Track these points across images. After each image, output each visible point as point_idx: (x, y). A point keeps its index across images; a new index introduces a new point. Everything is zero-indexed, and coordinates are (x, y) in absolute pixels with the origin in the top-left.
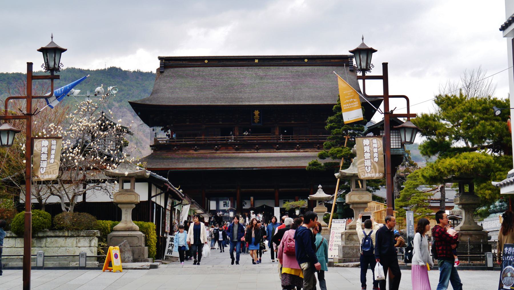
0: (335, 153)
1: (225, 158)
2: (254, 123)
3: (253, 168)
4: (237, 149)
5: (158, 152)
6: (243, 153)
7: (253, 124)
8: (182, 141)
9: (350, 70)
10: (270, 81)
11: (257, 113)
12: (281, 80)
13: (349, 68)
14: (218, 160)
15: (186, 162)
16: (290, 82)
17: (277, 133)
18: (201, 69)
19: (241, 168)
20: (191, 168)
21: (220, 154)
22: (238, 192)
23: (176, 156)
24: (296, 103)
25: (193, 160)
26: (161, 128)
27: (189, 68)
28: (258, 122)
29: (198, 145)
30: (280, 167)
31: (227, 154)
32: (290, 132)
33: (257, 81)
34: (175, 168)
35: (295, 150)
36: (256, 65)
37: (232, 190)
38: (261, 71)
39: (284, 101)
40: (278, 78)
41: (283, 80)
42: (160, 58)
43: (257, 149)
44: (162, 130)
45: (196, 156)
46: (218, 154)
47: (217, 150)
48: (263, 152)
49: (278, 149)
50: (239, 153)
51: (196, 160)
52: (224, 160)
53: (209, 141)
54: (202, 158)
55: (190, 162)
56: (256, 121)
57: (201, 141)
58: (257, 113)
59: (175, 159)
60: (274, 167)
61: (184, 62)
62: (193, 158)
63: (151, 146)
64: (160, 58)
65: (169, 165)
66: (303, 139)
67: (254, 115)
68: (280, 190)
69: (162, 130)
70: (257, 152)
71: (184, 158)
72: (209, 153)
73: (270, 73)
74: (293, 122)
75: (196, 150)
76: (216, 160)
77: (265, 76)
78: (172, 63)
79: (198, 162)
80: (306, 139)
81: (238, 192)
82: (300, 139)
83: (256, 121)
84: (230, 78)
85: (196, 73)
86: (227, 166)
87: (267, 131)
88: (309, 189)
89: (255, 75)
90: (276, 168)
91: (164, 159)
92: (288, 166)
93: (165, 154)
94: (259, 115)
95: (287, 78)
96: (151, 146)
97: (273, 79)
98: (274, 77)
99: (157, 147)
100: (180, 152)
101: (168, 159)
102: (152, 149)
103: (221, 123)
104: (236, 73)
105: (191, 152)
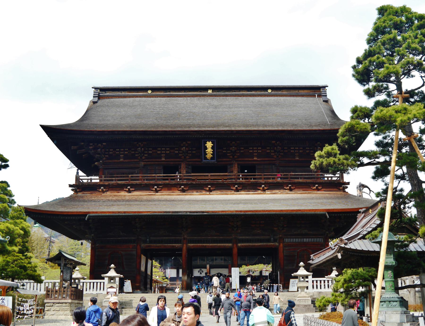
0: (390, 116)
1: (166, 200)
2: (206, 158)
3: (203, 212)
4: (183, 191)
5: (80, 194)
6: (191, 195)
7: (204, 161)
8: (113, 180)
9: (324, 101)
10: (227, 110)
11: (209, 145)
12: (241, 109)
13: (321, 99)
14: (157, 203)
15: (113, 205)
16: (251, 110)
17: (235, 172)
18: (144, 99)
19: (186, 212)
20: (119, 212)
21: (160, 197)
22: (184, 248)
23: (102, 198)
24: (261, 128)
25: (124, 203)
27: (129, 99)
28: (212, 158)
29: (132, 186)
30: (241, 211)
32: (252, 169)
33: (210, 110)
34: (96, 212)
35: (260, 192)
36: (210, 95)
37: (177, 245)
38: (216, 101)
39: (244, 126)
40: (236, 107)
41: (243, 109)
45: (127, 198)
46: (159, 196)
47: (157, 191)
50: (185, 195)
51: (127, 203)
52: (164, 203)
53: (147, 180)
54: (136, 200)
55: (118, 205)
56: (209, 156)
57: (138, 180)
58: (209, 145)
59: (99, 201)
60: (233, 211)
61: (123, 93)
62: (123, 201)
63: (70, 186)
64: (96, 88)
65: (89, 208)
66: (269, 179)
67: (206, 148)
68: (239, 245)
71: (112, 200)
72: (146, 195)
73: (227, 103)
74: (255, 159)
75: (129, 191)
76: (154, 203)
77: (221, 105)
79: (130, 205)
80: (273, 178)
81: (184, 248)
82: (265, 179)
83: (209, 156)
84: (177, 107)
85: (136, 103)
86: (168, 210)
87: (223, 169)
89: (208, 105)
90: (235, 213)
91: (84, 201)
92: (252, 209)
93: (87, 195)
94: (213, 148)
95: (248, 107)
96: (70, 186)
97: (230, 108)
98: (231, 106)
99: (79, 187)
100: (108, 193)
101: (91, 201)
102: (72, 190)
103: (163, 159)
104: (185, 103)
105: (123, 193)
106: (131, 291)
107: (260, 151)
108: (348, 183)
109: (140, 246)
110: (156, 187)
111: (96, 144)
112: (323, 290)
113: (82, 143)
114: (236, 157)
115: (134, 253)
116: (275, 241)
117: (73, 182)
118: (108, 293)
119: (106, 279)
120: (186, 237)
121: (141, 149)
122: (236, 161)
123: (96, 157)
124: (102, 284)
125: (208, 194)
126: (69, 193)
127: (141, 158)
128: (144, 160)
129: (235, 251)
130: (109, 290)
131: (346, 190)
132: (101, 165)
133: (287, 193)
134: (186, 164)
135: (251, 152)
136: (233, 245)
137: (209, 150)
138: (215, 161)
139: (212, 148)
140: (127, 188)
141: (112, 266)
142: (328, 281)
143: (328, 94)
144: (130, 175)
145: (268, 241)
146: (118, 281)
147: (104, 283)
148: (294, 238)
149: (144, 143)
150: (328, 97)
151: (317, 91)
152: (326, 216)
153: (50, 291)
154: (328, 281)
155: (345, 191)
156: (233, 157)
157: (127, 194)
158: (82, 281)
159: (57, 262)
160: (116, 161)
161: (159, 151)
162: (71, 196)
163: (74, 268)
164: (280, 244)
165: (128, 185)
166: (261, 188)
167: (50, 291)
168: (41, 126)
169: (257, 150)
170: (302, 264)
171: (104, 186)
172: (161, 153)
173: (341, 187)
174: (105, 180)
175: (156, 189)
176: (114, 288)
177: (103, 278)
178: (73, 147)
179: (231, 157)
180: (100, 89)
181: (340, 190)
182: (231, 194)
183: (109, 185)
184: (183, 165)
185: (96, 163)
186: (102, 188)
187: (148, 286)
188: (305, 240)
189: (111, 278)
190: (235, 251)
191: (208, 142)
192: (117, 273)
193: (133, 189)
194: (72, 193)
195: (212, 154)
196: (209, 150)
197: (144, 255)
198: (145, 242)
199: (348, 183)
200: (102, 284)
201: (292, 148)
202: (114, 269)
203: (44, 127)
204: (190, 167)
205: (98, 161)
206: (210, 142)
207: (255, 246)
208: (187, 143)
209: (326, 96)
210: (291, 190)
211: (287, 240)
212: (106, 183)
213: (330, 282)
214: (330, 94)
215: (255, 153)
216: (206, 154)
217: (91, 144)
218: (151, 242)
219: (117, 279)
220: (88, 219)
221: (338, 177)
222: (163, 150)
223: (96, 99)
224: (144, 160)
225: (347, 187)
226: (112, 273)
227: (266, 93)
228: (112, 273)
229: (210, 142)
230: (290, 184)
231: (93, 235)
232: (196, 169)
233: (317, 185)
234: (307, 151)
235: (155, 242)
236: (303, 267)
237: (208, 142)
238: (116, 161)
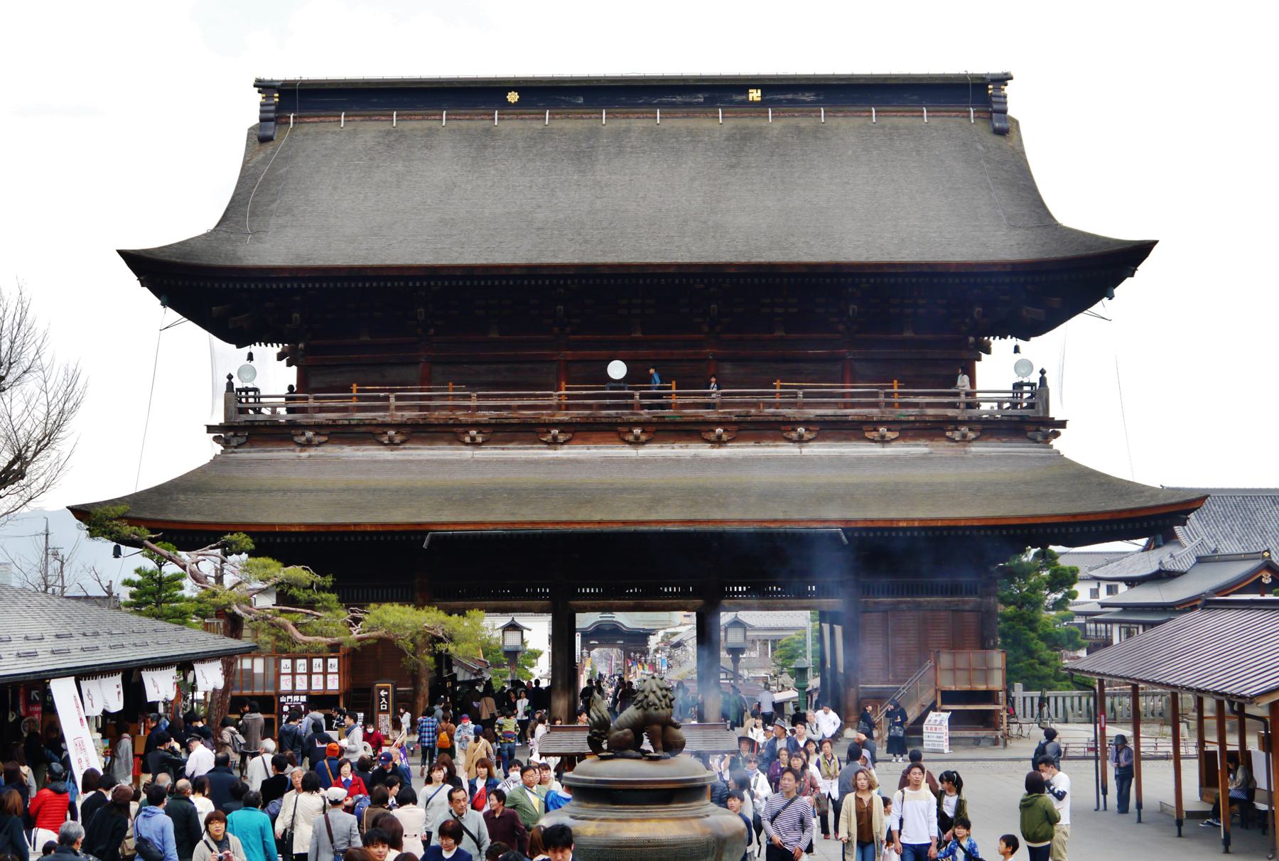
26: (276, 349)
42: (262, 86)
44: (280, 357)
63: (210, 429)
64: (262, 86)
69: (280, 357)
102: (215, 439)
107: (795, 310)
108: (1063, 424)
110: (473, 433)
117: (219, 419)
126: (207, 450)
131: (1056, 443)
143: (1008, 105)
150: (1011, 112)
151: (977, 96)
162: (215, 461)
171: (318, 428)
180: (279, 91)
194: (218, 448)
199: (1063, 424)
203: (123, 254)
209: (1005, 112)
214: (1017, 101)
225: (1057, 435)
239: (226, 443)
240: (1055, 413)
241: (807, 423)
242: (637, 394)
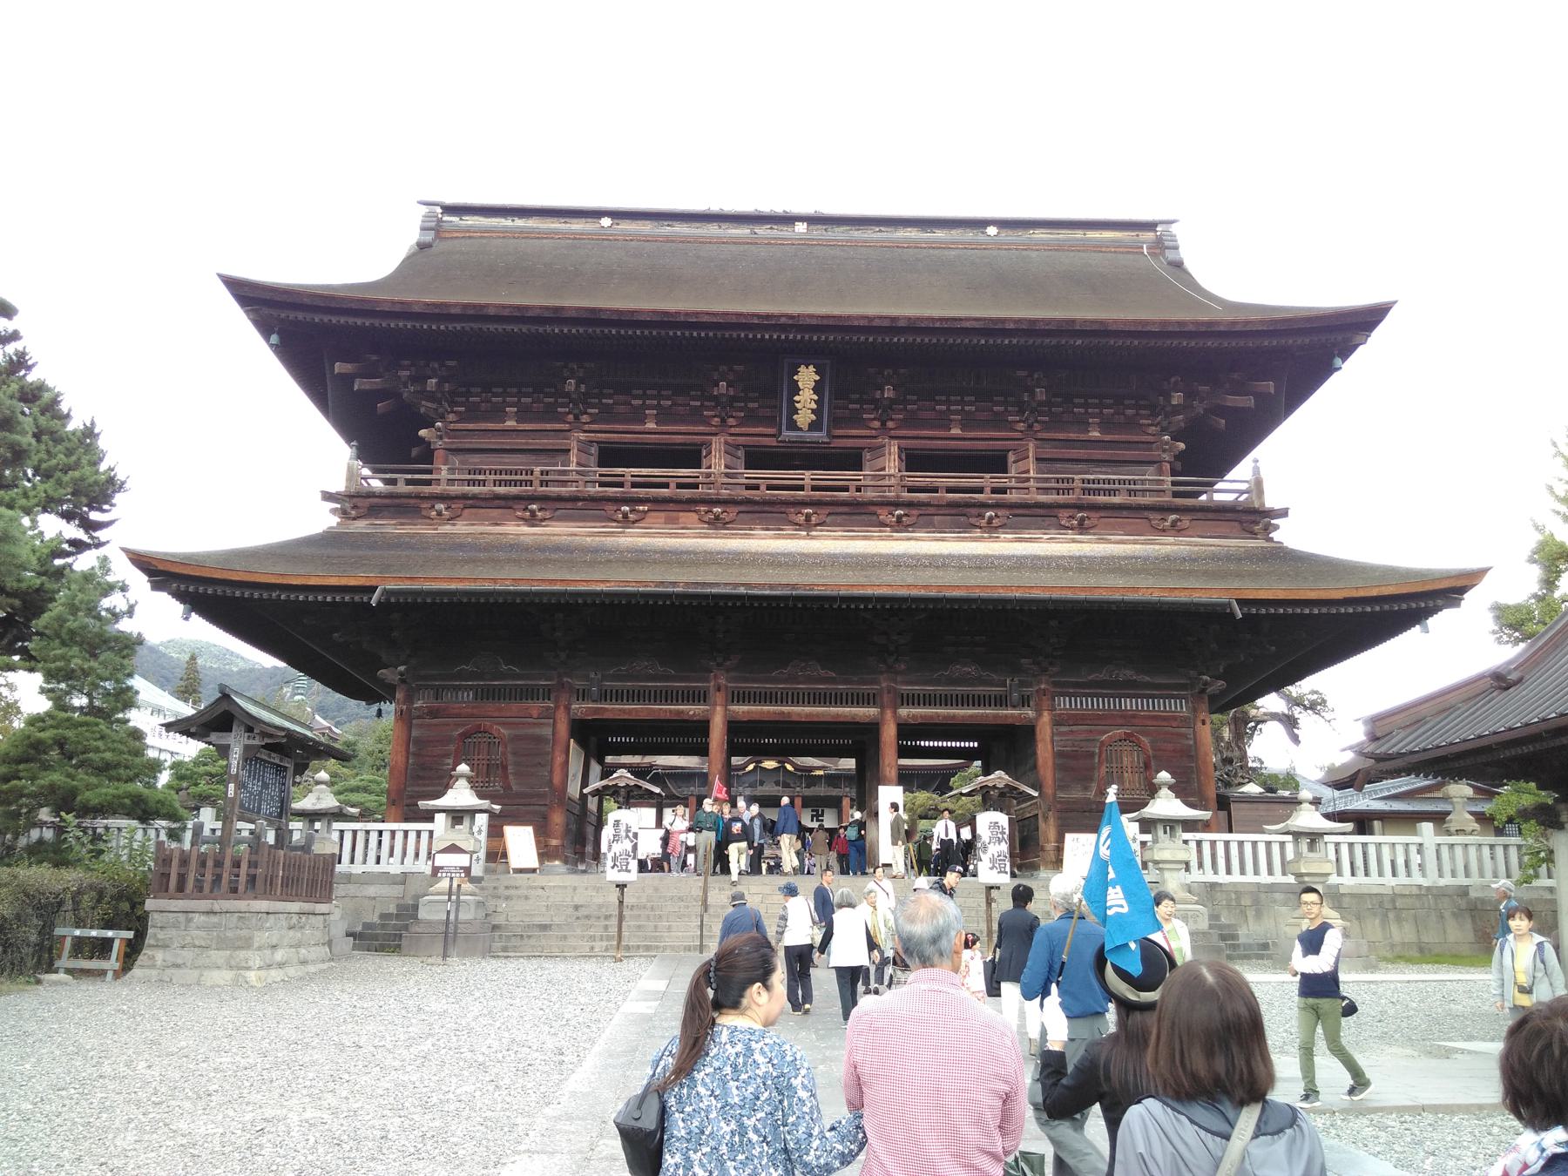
2: (793, 426)
4: (717, 524)
11: (807, 377)
19: (737, 585)
28: (814, 426)
31: (674, 541)
35: (977, 533)
43: (808, 525)
47: (626, 521)
48: (835, 538)
49: (900, 526)
56: (804, 417)
57: (564, 483)
58: (807, 377)
63: (328, 496)
67: (795, 389)
68: (903, 712)
70: (813, 538)
75: (532, 520)
78: (471, 221)
83: (804, 417)
87: (853, 460)
88: (1031, 713)
94: (817, 389)
96: (328, 496)
99: (353, 503)
100: (461, 528)
102: (334, 511)
103: (651, 425)
106: (535, 863)
109: (568, 708)
111: (422, 363)
112: (1222, 878)
113: (374, 358)
114: (890, 424)
115: (547, 731)
116: (1024, 702)
117: (339, 485)
118: (436, 870)
119: (440, 817)
120: (722, 681)
121: (578, 386)
122: (892, 437)
123: (422, 410)
124: (425, 836)
125: (804, 538)
127: (576, 418)
128: (586, 427)
129: (889, 733)
130: (441, 860)
131: (1275, 535)
132: (441, 438)
133: (1074, 541)
134: (726, 443)
135: (941, 412)
136: (882, 713)
137: (806, 399)
138: (824, 433)
139: (816, 390)
140: (526, 509)
141: (463, 768)
142: (1282, 844)
144: (537, 469)
145: (1001, 701)
146: (485, 829)
147: (431, 833)
148: (1087, 695)
149: (587, 365)
152: (1232, 614)
153: (175, 863)
154: (1282, 844)
155: (1271, 540)
156: (883, 424)
157: (526, 529)
158: (337, 826)
159: (214, 737)
160: (491, 426)
161: (636, 397)
163: (301, 769)
164: (1040, 715)
165: (533, 499)
166: (983, 522)
167: (175, 863)
168: (220, 276)
169: (962, 403)
170: (1164, 776)
172: (644, 407)
173: (1257, 523)
174: (451, 482)
175: (625, 516)
176: (463, 851)
177: (428, 816)
178: (339, 367)
179: (877, 424)
181: (1253, 535)
182: (881, 538)
183: (464, 497)
184: (717, 444)
185: (422, 433)
186: (440, 506)
187: (589, 849)
188: (1128, 704)
189: (458, 816)
190: (889, 733)
191: (802, 369)
192: (481, 796)
193: (548, 514)
194: (333, 521)
195: (813, 411)
196: (806, 399)
197: (582, 743)
198: (583, 695)
199: (1284, 513)
200: (425, 836)
201: (1076, 401)
202: (469, 779)
204: (741, 453)
205: (429, 424)
206: (811, 368)
207: (954, 717)
208: (731, 370)
209: (1176, 248)
210: (1082, 528)
211: (1064, 703)
212: (456, 489)
213: (1290, 848)
215: (956, 412)
216: (796, 411)
217: (406, 362)
218: (604, 696)
219: (482, 820)
220: (379, 603)
221: (1242, 492)
222: (652, 397)
223: (429, 237)
224: (586, 427)
225: (1276, 527)
226: (461, 795)
227: (981, 237)
228: (461, 795)
229: (811, 368)
230: (1080, 507)
231: (402, 668)
232: (756, 459)
233: (1174, 517)
234: (1130, 412)
235: (618, 696)
236: (1171, 788)
237: (802, 369)
238: (491, 426)
239: (344, 513)
240: (1271, 502)
241: (997, 506)
242: (808, 475)
